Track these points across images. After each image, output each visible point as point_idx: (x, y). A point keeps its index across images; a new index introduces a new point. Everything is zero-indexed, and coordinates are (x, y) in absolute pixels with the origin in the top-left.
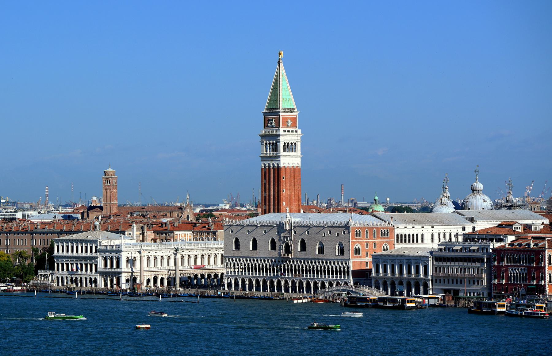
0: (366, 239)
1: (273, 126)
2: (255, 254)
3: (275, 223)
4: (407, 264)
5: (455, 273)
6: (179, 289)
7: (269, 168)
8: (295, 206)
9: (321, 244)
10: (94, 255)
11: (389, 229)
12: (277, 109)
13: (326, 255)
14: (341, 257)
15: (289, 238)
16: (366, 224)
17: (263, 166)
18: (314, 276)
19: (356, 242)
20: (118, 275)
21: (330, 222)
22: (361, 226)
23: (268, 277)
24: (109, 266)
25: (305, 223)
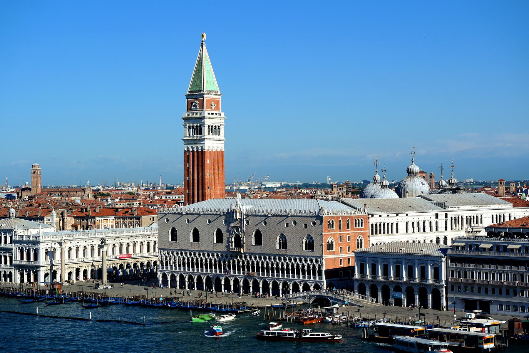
0: (339, 231)
1: (196, 109)
2: (196, 247)
3: (221, 210)
4: (407, 265)
5: (483, 279)
6: (107, 287)
7: (193, 151)
8: (219, 190)
9: (283, 236)
10: (9, 246)
11: (363, 218)
12: (201, 91)
13: (291, 249)
14: (310, 253)
15: (239, 229)
16: (339, 213)
17: (186, 149)
18: (273, 275)
20: (35, 269)
21: (295, 211)
22: (334, 215)
23: (213, 274)
24: (25, 258)
25: (261, 211)
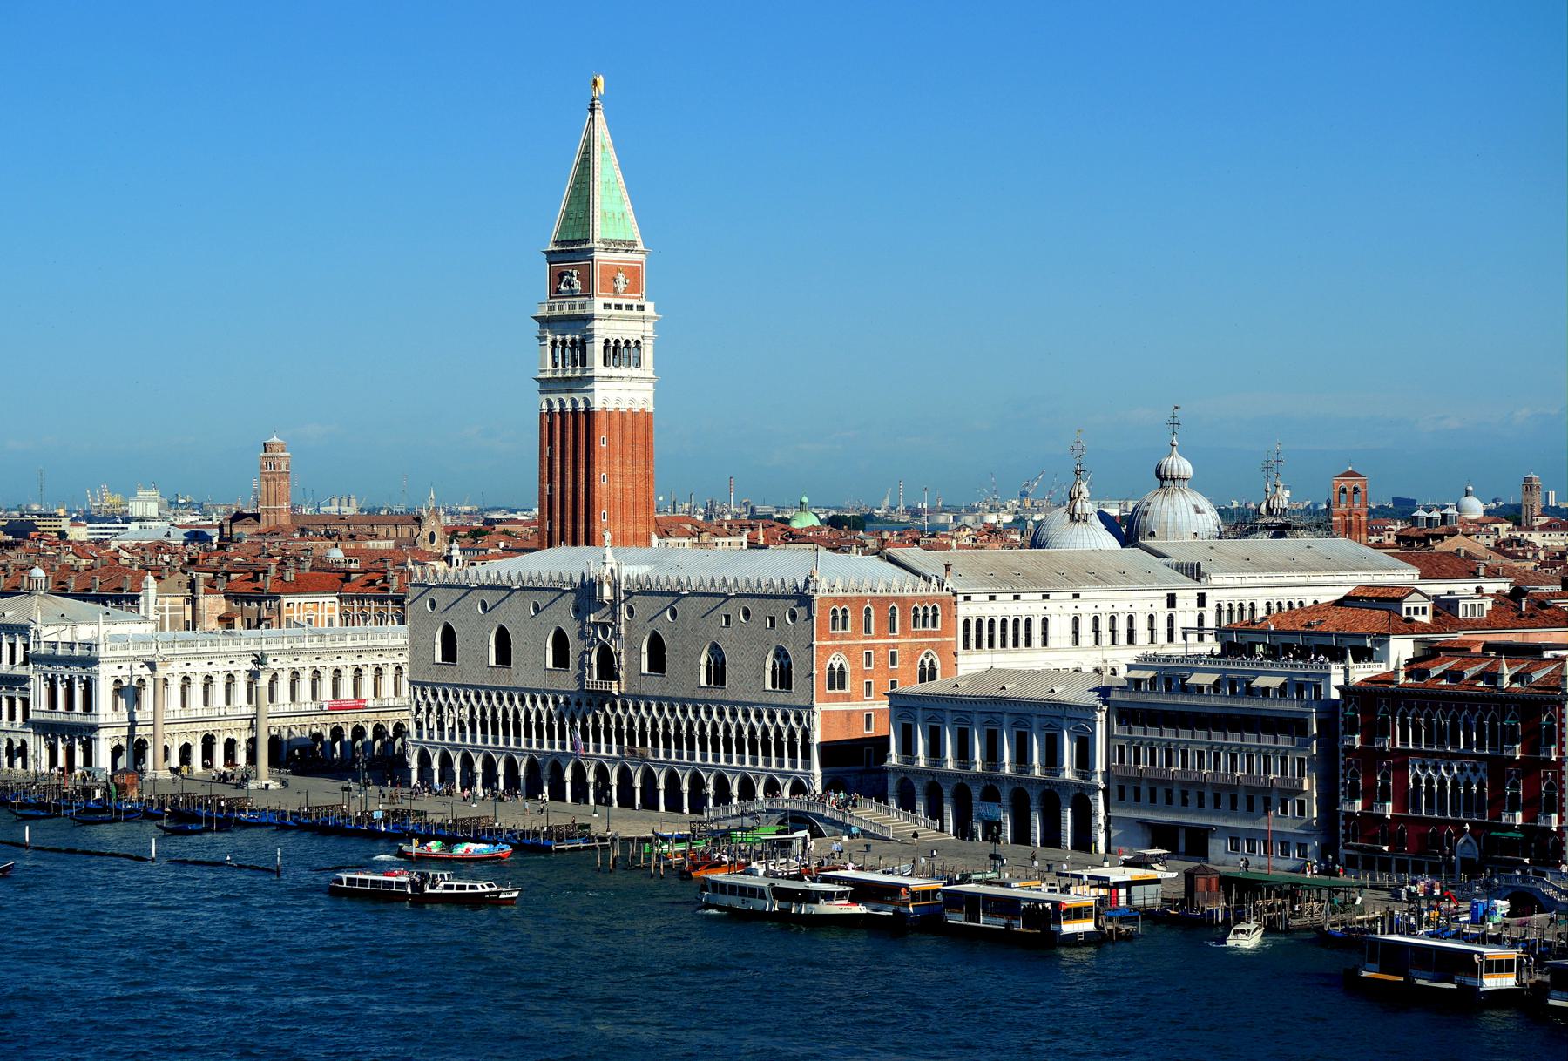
0: (865, 638)
1: (572, 291)
2: (503, 678)
3: (566, 579)
4: (1015, 730)
5: (1194, 768)
6: (267, 785)
7: (563, 412)
8: (635, 523)
9: (716, 651)
10: (19, 670)
11: (940, 602)
12: (587, 241)
13: (735, 689)
14: (781, 697)
15: (610, 630)
16: (864, 587)
17: (545, 406)
18: (691, 757)
19: (834, 648)
20: (86, 734)
21: (748, 581)
22: (848, 594)
23: (545, 752)
24: (61, 706)
25: (663, 582)
